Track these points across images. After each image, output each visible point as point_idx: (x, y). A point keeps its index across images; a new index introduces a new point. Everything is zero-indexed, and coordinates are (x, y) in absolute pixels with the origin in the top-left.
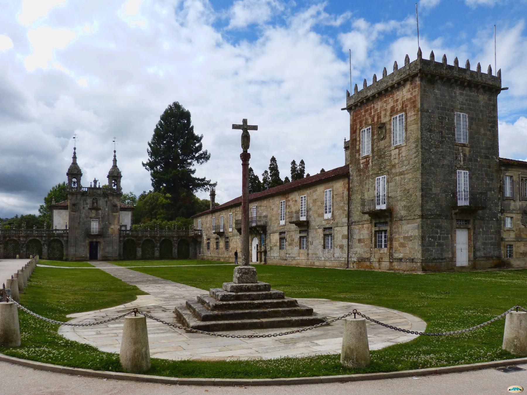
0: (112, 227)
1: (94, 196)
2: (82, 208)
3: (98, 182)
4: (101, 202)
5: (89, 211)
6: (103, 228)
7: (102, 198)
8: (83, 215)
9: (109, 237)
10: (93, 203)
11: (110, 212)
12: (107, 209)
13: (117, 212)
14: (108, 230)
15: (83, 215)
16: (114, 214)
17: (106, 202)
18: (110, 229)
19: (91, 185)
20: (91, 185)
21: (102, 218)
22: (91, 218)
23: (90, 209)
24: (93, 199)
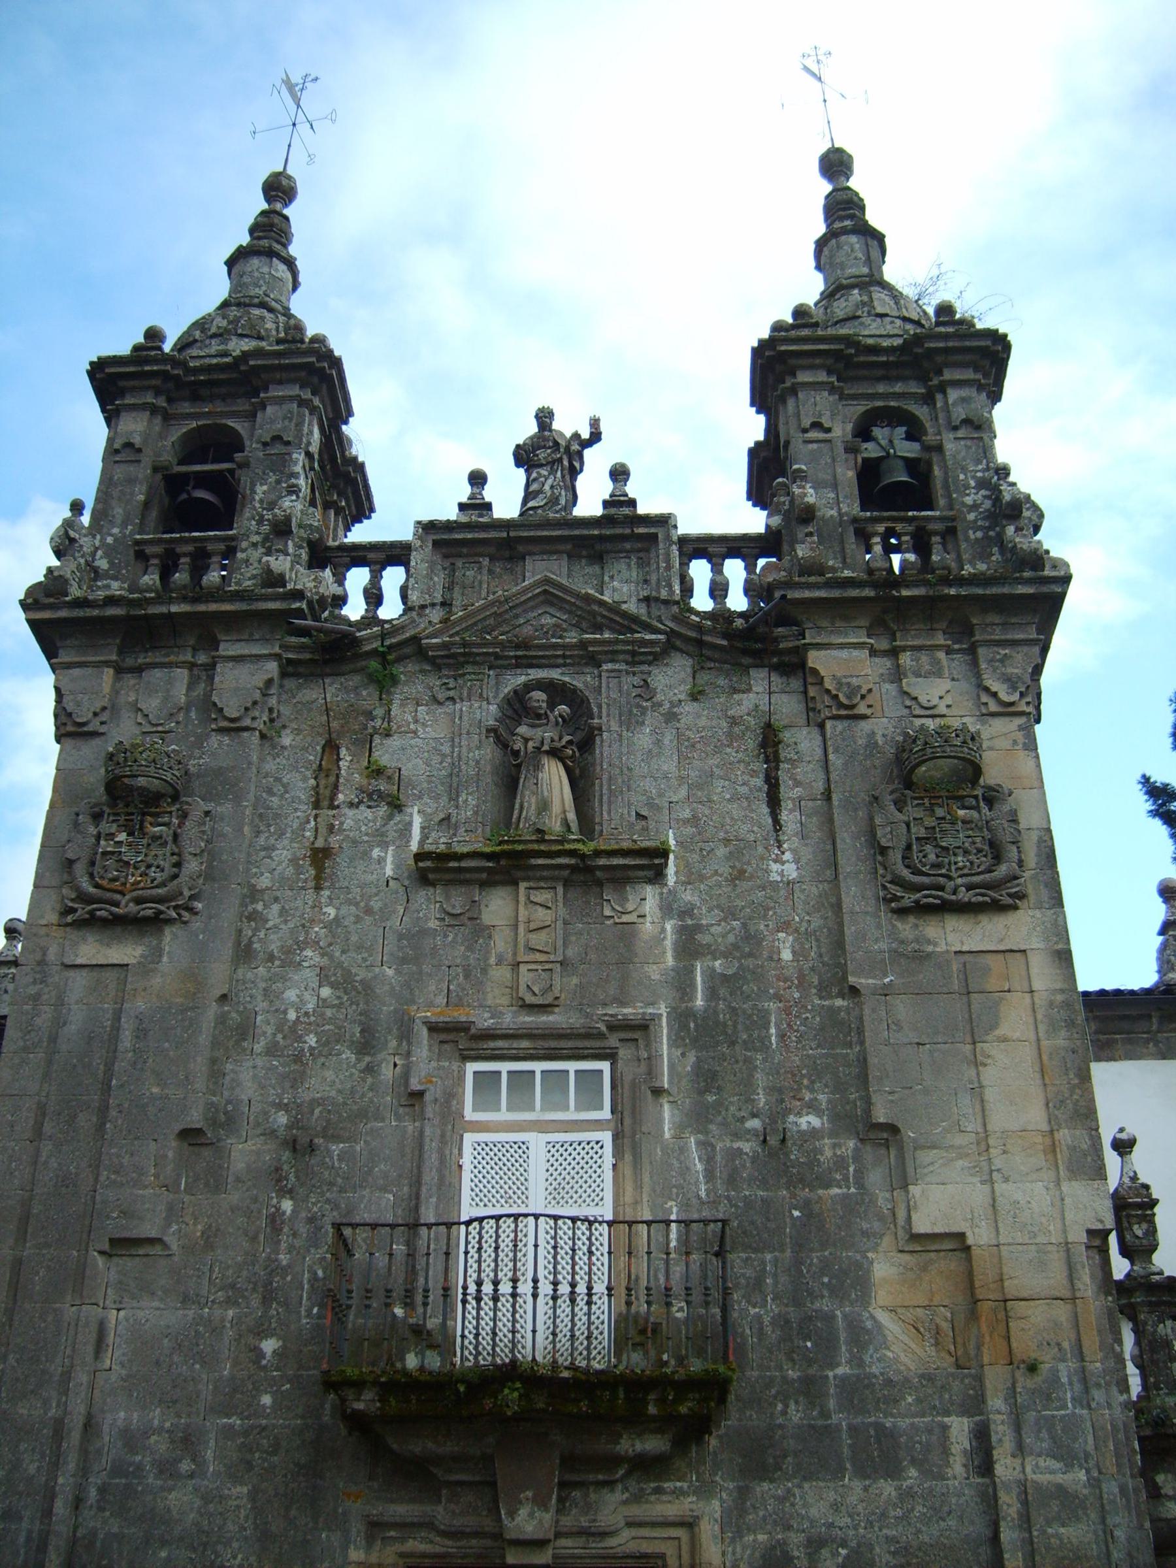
0: (942, 1199)
1: (523, 654)
2: (286, 854)
3: (597, 463)
4: (671, 758)
5: (429, 906)
6: (718, 1240)
7: (672, 678)
8: (302, 993)
9: (880, 1455)
10: (511, 776)
11: (857, 896)
12: (785, 868)
13: (996, 899)
14: (854, 1282)
15: (302, 993)
16: (953, 936)
17: (770, 742)
18: (885, 1267)
19: (476, 506)
20: (476, 506)
21: (697, 1031)
22: (462, 1039)
23: (434, 869)
24: (517, 707)
